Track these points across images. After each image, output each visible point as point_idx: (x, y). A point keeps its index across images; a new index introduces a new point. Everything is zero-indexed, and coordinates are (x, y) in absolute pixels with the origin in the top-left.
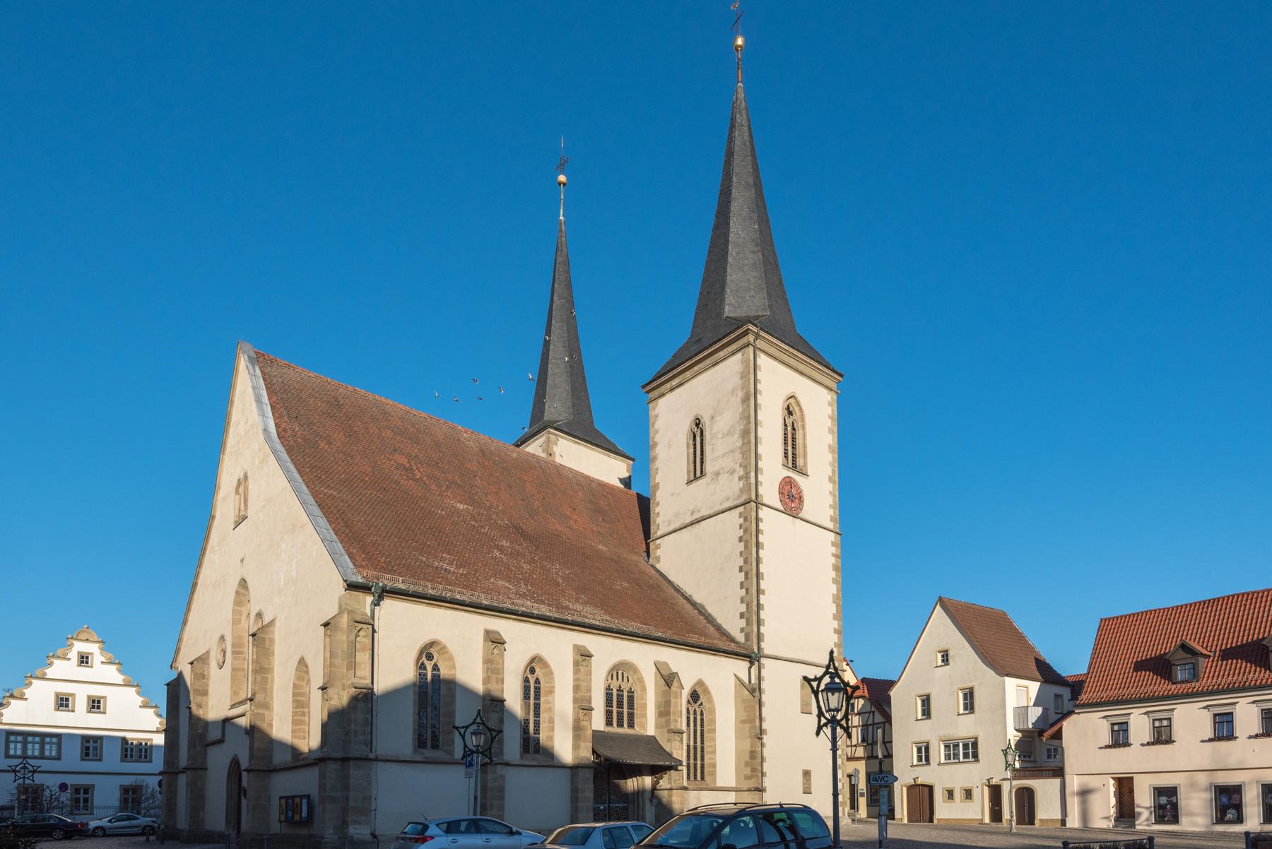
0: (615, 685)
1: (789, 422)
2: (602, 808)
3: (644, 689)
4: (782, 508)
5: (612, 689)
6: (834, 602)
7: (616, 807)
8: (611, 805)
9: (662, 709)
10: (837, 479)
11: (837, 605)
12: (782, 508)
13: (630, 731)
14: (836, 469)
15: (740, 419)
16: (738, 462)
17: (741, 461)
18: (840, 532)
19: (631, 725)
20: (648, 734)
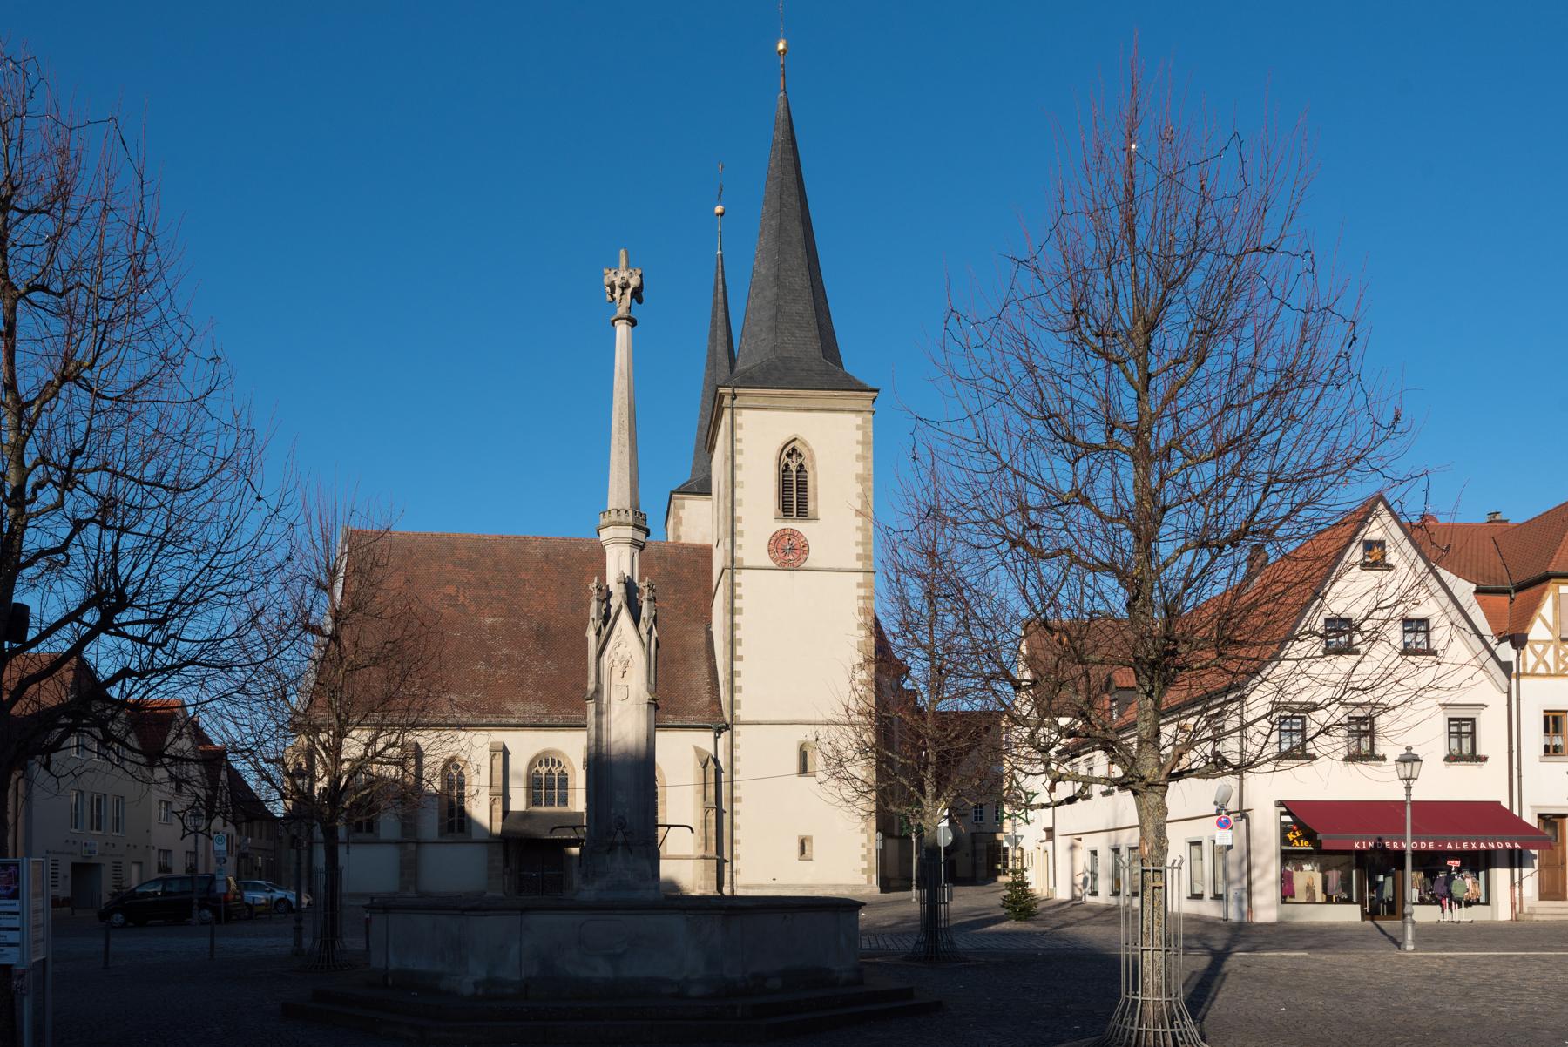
0: (543, 770)
1: (793, 467)
4: (773, 565)
12: (773, 565)
13: (562, 809)
14: (871, 499)
19: (566, 804)
20: (577, 810)
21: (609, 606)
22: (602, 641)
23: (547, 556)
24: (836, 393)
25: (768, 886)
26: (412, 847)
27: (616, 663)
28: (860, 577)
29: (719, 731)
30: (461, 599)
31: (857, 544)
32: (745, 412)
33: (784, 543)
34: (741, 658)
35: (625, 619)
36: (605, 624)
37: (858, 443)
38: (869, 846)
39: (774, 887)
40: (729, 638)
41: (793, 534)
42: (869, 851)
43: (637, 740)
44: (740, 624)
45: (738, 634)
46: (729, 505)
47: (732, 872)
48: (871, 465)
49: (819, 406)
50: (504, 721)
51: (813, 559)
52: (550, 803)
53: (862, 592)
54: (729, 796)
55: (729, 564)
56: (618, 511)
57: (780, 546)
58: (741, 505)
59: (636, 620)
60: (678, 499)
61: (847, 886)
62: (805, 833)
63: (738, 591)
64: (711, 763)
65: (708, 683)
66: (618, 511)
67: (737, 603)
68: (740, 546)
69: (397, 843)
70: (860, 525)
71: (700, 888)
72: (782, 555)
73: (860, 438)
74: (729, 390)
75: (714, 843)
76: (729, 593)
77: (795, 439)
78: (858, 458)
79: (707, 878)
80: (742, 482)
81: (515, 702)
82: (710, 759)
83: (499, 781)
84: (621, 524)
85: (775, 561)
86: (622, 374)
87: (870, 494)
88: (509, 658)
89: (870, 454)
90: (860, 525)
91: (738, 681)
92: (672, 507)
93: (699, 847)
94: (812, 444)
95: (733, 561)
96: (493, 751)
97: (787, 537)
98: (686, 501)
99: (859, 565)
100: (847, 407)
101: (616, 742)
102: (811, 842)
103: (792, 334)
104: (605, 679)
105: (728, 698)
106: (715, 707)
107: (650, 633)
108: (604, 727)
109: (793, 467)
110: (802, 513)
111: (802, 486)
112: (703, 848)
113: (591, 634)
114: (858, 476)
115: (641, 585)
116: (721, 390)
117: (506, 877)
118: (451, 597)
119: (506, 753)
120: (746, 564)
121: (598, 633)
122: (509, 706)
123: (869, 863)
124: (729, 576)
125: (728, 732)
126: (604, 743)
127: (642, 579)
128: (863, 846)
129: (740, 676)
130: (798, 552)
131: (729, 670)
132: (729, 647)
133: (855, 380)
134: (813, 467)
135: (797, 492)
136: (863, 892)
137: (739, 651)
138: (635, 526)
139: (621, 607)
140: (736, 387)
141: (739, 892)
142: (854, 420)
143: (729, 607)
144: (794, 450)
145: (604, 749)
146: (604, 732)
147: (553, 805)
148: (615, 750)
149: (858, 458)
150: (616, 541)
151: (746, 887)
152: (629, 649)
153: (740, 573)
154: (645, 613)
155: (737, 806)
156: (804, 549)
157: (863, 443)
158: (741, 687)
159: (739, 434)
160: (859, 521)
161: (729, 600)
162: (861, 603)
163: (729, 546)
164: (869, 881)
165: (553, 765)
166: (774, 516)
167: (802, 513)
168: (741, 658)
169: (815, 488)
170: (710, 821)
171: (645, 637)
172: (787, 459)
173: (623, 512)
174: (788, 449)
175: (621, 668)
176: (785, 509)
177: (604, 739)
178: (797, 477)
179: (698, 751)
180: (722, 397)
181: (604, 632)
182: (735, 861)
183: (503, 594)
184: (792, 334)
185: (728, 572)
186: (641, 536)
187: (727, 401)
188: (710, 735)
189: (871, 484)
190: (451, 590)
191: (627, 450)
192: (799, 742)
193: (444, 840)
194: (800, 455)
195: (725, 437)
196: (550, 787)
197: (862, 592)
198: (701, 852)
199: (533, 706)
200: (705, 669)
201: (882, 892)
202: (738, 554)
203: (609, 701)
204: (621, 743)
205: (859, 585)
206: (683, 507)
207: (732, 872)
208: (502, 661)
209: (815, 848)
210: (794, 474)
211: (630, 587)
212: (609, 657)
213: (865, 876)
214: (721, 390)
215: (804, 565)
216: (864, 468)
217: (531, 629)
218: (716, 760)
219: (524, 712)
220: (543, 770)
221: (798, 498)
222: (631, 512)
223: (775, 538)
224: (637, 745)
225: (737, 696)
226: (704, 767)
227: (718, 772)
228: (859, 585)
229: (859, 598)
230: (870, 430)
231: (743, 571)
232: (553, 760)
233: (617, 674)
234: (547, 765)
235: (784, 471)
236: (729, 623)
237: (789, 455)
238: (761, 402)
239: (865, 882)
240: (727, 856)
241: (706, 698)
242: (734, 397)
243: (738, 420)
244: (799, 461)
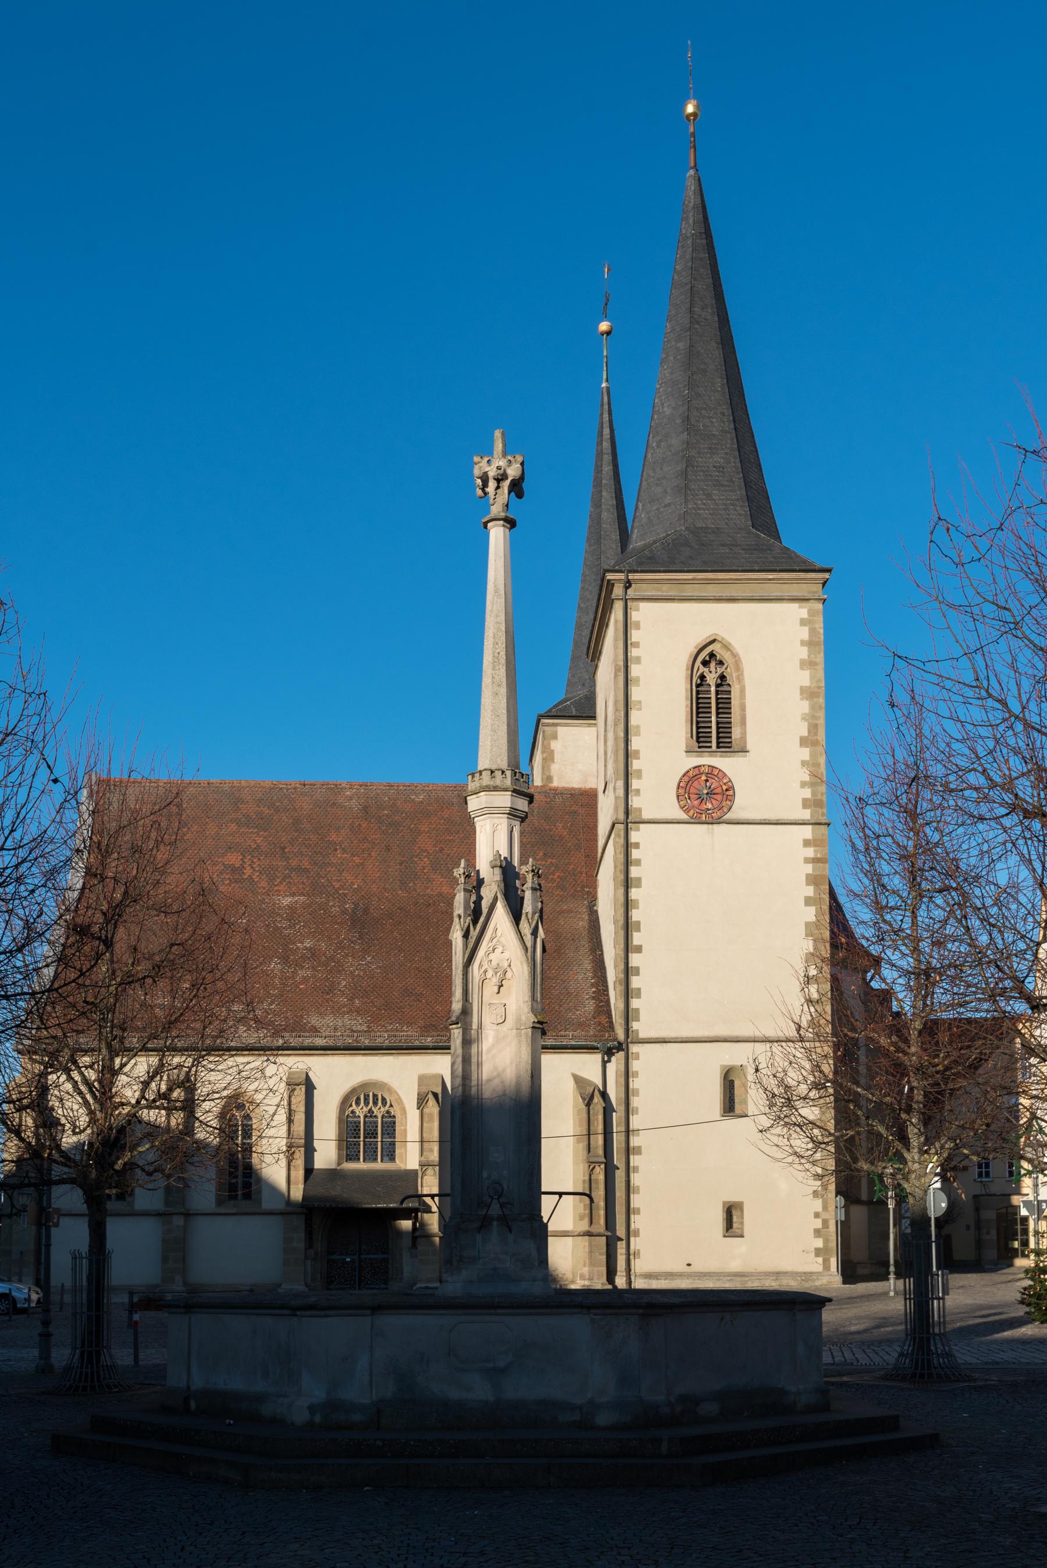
0: (361, 1111)
1: (712, 679)
2: (348, 1260)
3: (404, 1111)
4: (683, 816)
7: (370, 1259)
8: (362, 1256)
10: (821, 736)
11: (815, 941)
12: (683, 816)
14: (821, 722)
18: (824, 820)
19: (392, 1158)
21: (480, 898)
22: (471, 945)
23: (366, 809)
24: (771, 576)
25: (680, 1275)
26: (179, 1221)
27: (490, 974)
28: (807, 832)
29: (609, 1053)
30: (248, 871)
31: (803, 784)
32: (643, 605)
33: (700, 785)
34: (639, 949)
35: (501, 916)
36: (475, 922)
37: (803, 643)
38: (825, 1216)
39: (689, 1275)
40: (622, 922)
41: (712, 772)
42: (825, 1223)
43: (518, 1077)
44: (637, 901)
45: (635, 915)
46: (622, 734)
47: (628, 1254)
48: (821, 674)
49: (747, 594)
50: (307, 1042)
51: (743, 805)
52: (370, 1156)
53: (810, 852)
54: (623, 1145)
55: (621, 816)
56: (492, 772)
57: (692, 790)
58: (638, 734)
59: (516, 916)
60: (548, 725)
61: (793, 1274)
63: (635, 854)
64: (597, 1099)
65: (592, 985)
66: (492, 772)
67: (634, 872)
68: (638, 792)
69: (159, 1214)
71: (582, 1277)
72: (696, 803)
74: (621, 576)
75: (602, 1212)
76: (621, 857)
77: (714, 641)
78: (804, 664)
79: (592, 1263)
80: (640, 702)
81: (322, 1015)
82: (597, 1095)
83: (299, 1127)
84: (496, 789)
85: (687, 811)
86: (496, 591)
87: (821, 714)
88: (313, 953)
89: (820, 658)
91: (635, 982)
92: (540, 737)
93: (581, 1218)
94: (737, 646)
95: (627, 813)
96: (292, 1085)
97: (704, 778)
98: (559, 728)
99: (806, 814)
100: (786, 594)
101: (489, 1081)
102: (742, 1211)
103: (709, 496)
104: (475, 996)
105: (621, 1006)
106: (604, 1019)
107: (535, 933)
108: (474, 1060)
109: (712, 679)
110: (725, 742)
111: (724, 705)
112: (586, 1221)
113: (456, 936)
114: (803, 690)
115: (524, 870)
116: (610, 576)
117: (309, 1262)
118: (234, 870)
119: (310, 1087)
120: (645, 816)
121: (466, 935)
122: (314, 1020)
123: (826, 1241)
124: (622, 833)
125: (621, 1054)
126: (474, 1083)
127: (523, 862)
128: (817, 1215)
129: (638, 974)
130: (719, 797)
131: (622, 966)
132: (622, 933)
133: (798, 556)
134: (740, 679)
135: (718, 713)
136: (818, 1283)
137: (637, 939)
138: (514, 791)
139: (495, 899)
140: (630, 571)
141: (639, 1284)
142: (798, 611)
143: (622, 877)
144: (712, 655)
145: (474, 1090)
146: (474, 1067)
147: (375, 1160)
148: (487, 1093)
149: (804, 664)
150: (489, 811)
151: (649, 1276)
152: (506, 955)
153: (638, 830)
154: (528, 907)
155: (635, 1160)
156: (727, 793)
157: (810, 644)
158: (639, 989)
159: (635, 636)
160: (805, 753)
161: (622, 867)
162: (809, 869)
163: (621, 792)
164: (826, 1266)
165: (375, 1103)
166: (685, 749)
167: (725, 742)
168: (639, 949)
169: (743, 708)
170: (597, 1181)
171: (528, 939)
172: (702, 669)
173: (498, 774)
175: (495, 980)
176: (700, 738)
177: (474, 1077)
178: (717, 693)
179: (578, 1080)
180: (611, 585)
181: (474, 934)
182: (632, 1239)
183: (306, 864)
184: (709, 496)
185: (620, 827)
186: (522, 804)
187: (618, 591)
188: (596, 1058)
189: (821, 700)
190: (233, 859)
191: (503, 690)
193: (222, 1211)
194: (721, 663)
195: (616, 640)
196: (371, 1134)
197: (810, 852)
198: (584, 1226)
199: (347, 1021)
200: (587, 965)
201: (844, 1283)
202: (635, 802)
203: (480, 1026)
204: (496, 1082)
205: (807, 843)
206: (555, 737)
207: (628, 1254)
208: (304, 958)
209: (749, 1220)
210: (713, 689)
211: (508, 872)
212: (481, 966)
213: (820, 1260)
214: (610, 576)
215: (729, 816)
216: (812, 677)
217: (344, 912)
218: (604, 1095)
219: (335, 1029)
220: (361, 1111)
221: (718, 723)
222: (509, 773)
223: (686, 779)
224: (518, 1084)
225: (635, 1003)
226: (588, 1105)
227: (608, 1111)
228: (807, 843)
229: (807, 860)
230: (819, 626)
231: (642, 826)
232: (375, 1096)
233: (490, 988)
234: (367, 1103)
235: (698, 686)
236: (621, 899)
237: (705, 663)
238: (666, 590)
239: (820, 1268)
240: (621, 1232)
241: (590, 1006)
242: (628, 585)
243: (634, 616)
244: (720, 671)
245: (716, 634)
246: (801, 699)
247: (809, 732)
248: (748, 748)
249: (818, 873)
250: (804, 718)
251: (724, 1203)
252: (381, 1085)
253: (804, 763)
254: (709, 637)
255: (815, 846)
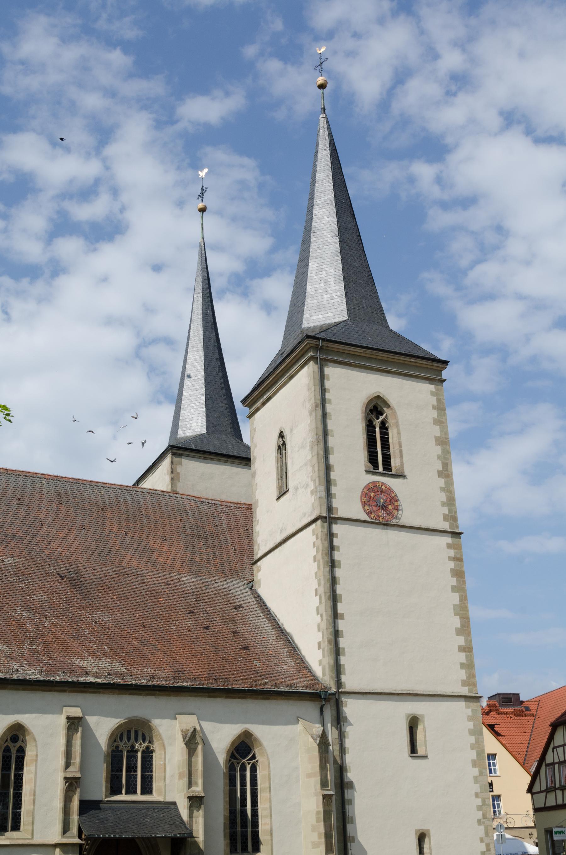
5: (121, 751)
6: (455, 614)
9: (181, 770)
11: (461, 618)
15: (309, 431)
16: (310, 475)
17: (311, 474)
31: (443, 504)
37: (434, 407)
38: (487, 840)
52: (131, 790)
62: (423, 827)
70: (443, 486)
73: (435, 403)
90: (443, 486)
120: (341, 513)
131: (331, 630)
132: (330, 603)
147: (135, 792)
161: (328, 551)
174: (371, 406)
192: (408, 715)
202: (335, 503)
205: (449, 546)
229: (450, 559)
231: (338, 521)
232: (136, 732)
234: (129, 739)
236: (328, 576)
245: (379, 392)
246: (436, 445)
247: (443, 467)
248: (406, 473)
249: (458, 569)
250: (439, 457)
251: (417, 831)
252: (144, 722)
253: (442, 489)
254: (375, 393)
255: (454, 549)
